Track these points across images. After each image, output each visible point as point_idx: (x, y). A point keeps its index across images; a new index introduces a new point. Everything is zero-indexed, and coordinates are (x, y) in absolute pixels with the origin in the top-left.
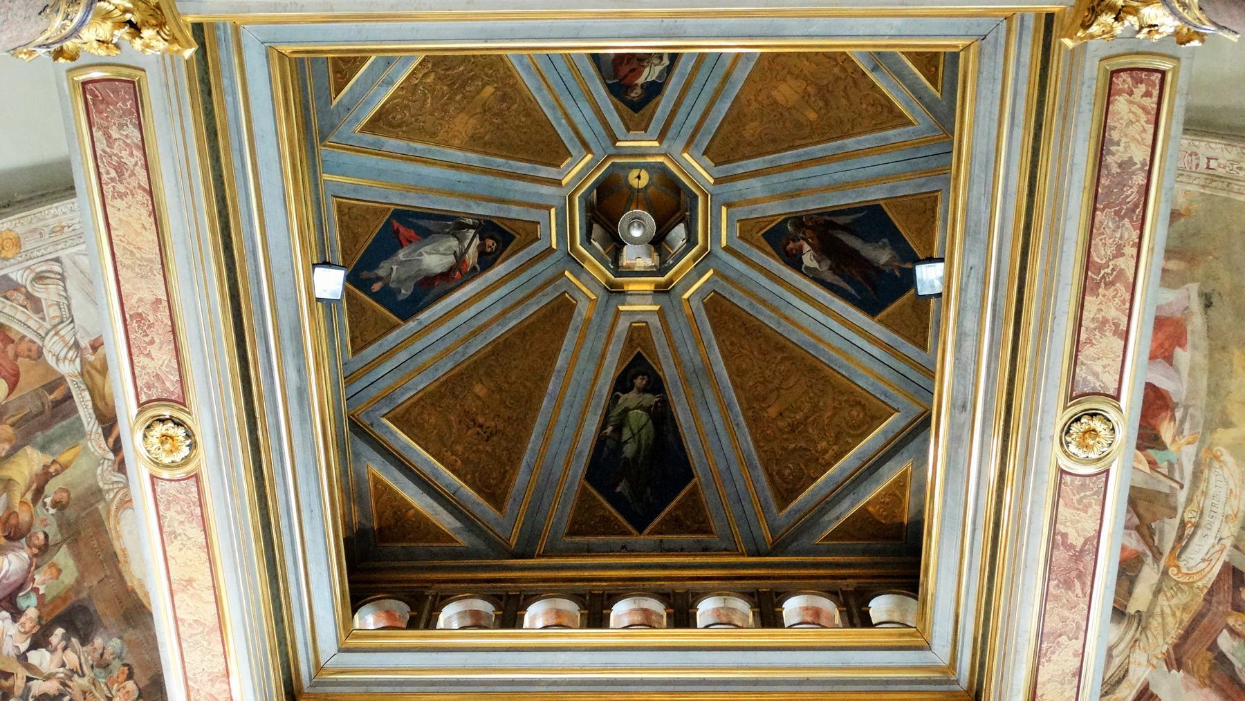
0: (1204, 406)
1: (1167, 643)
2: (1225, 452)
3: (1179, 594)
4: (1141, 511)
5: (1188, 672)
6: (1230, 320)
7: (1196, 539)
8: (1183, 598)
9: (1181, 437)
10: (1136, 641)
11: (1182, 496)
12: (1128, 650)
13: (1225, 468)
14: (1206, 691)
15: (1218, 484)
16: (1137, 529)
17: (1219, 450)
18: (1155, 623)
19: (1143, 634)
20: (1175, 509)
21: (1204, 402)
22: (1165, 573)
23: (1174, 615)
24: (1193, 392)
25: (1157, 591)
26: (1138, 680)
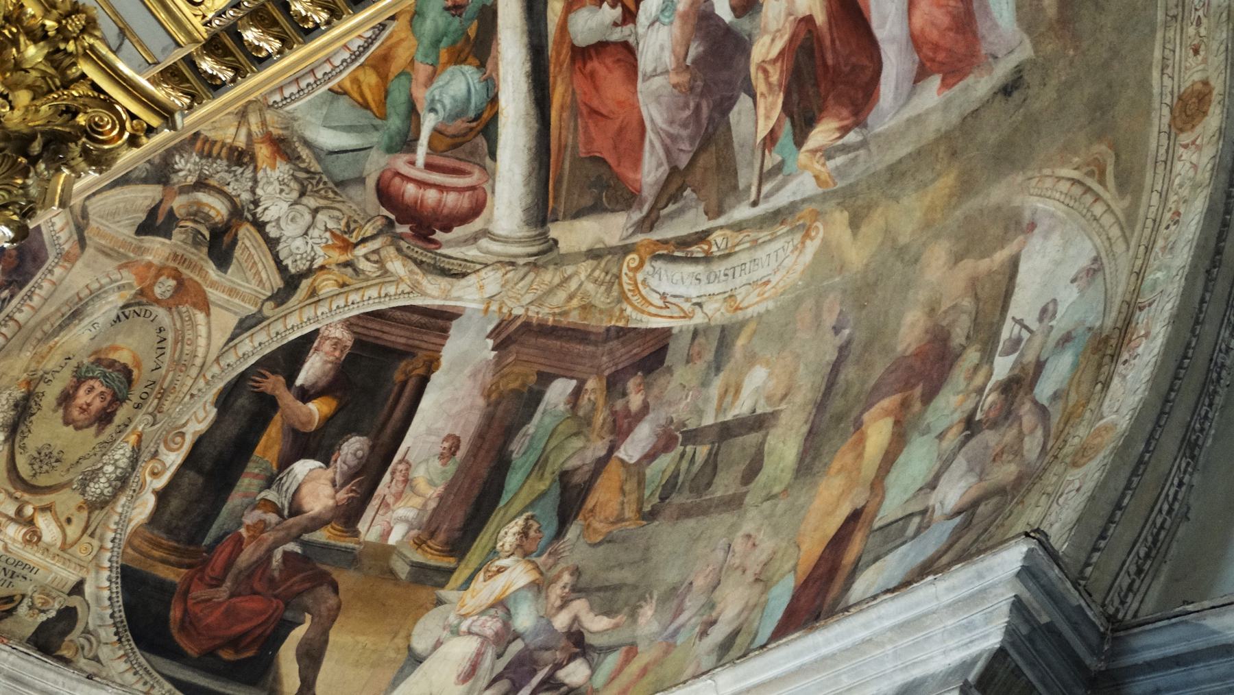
0: (872, 170)
1: (527, 310)
2: (817, 242)
3: (603, 288)
4: (701, 162)
5: (498, 362)
6: (993, 138)
7: (689, 269)
8: (600, 298)
9: (822, 160)
10: (513, 264)
11: (742, 212)
12: (495, 259)
13: (796, 253)
14: (481, 402)
15: (773, 257)
16: (674, 170)
18: (549, 277)
19: (526, 269)
20: (720, 212)
21: (879, 167)
22: (626, 250)
24: (888, 139)
25: (594, 254)
26: (459, 299)
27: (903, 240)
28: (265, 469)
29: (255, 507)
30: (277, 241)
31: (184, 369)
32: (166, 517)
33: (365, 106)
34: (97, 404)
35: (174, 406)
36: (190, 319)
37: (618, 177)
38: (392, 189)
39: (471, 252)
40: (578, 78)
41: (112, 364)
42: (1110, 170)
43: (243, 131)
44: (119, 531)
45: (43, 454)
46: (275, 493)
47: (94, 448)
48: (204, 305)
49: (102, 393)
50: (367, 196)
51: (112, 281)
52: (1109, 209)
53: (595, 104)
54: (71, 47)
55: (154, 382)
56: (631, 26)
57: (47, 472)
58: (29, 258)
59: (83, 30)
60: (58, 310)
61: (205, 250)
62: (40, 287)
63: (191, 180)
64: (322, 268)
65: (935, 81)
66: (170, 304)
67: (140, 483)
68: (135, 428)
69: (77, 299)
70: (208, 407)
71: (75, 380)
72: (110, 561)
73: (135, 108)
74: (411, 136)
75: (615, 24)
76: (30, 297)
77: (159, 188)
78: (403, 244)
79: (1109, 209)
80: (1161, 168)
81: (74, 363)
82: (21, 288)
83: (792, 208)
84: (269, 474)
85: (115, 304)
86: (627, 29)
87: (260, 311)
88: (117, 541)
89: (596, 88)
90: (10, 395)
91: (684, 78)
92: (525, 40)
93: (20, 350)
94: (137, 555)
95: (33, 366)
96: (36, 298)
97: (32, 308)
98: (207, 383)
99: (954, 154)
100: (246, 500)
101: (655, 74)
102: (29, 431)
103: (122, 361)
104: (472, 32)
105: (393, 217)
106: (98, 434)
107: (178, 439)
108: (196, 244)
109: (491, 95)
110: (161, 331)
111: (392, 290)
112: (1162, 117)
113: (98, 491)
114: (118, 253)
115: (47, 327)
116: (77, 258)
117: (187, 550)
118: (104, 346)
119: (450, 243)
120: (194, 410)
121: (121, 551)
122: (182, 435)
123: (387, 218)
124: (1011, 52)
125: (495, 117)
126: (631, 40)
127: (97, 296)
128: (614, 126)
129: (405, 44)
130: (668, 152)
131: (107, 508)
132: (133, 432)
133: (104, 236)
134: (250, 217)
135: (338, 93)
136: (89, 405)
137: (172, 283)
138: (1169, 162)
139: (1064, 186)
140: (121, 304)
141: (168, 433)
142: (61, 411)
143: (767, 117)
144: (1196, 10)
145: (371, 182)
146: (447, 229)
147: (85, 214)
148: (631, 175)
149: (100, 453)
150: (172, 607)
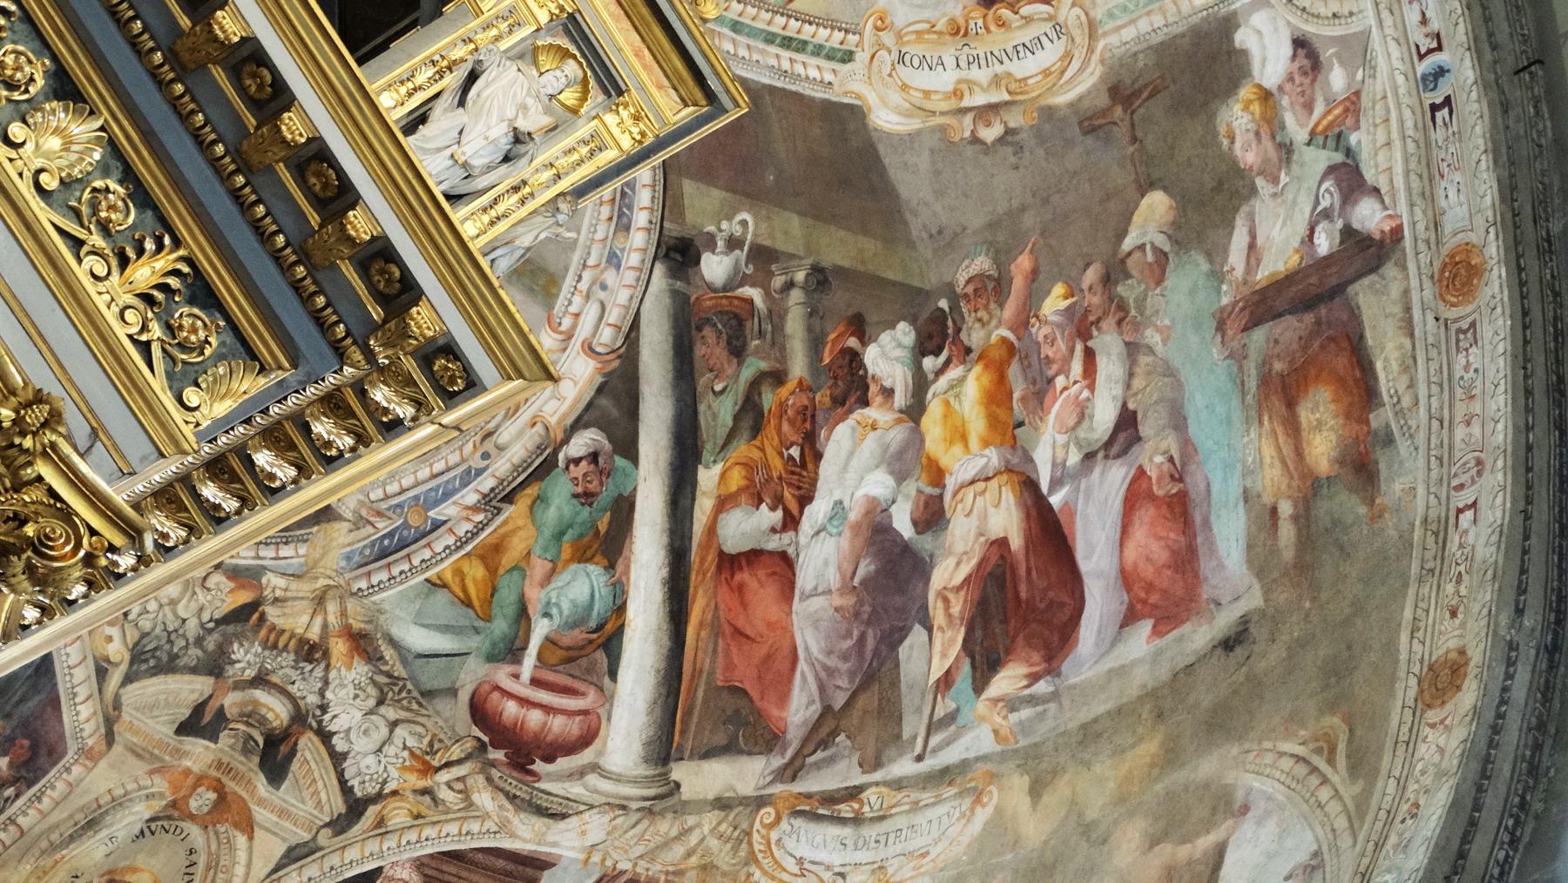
0: (1062, 729)
1: (635, 865)
2: (989, 810)
3: (729, 846)
4: (861, 702)
9: (1004, 712)
10: (624, 807)
11: (904, 767)
12: (604, 800)
13: (963, 821)
15: (935, 825)
16: (827, 710)
17: (993, 797)
18: (666, 826)
19: (639, 815)
20: (877, 765)
21: (1070, 725)
22: (760, 802)
23: (689, 854)
24: (1085, 692)
25: (722, 804)
26: (555, 844)
27: (1091, 814)
30: (344, 756)
33: (467, 603)
36: (229, 841)
37: (759, 714)
38: (488, 705)
39: (575, 790)
40: (724, 591)
42: (1342, 747)
43: (318, 621)
48: (247, 826)
50: (459, 711)
51: (140, 788)
52: (1337, 794)
53: (740, 622)
54: (28, 442)
56: (791, 534)
58: (43, 751)
59: (45, 425)
60: (71, 816)
61: (256, 759)
62: (53, 787)
63: (250, 674)
64: (395, 793)
65: (1146, 626)
66: (206, 822)
73: (96, 522)
74: (518, 644)
75: (773, 530)
76: (39, 799)
77: (210, 680)
78: (495, 773)
79: (1337, 794)
80: (1401, 749)
82: (29, 787)
83: (964, 766)
86: (788, 537)
87: (314, 839)
89: (744, 605)
91: (849, 601)
92: (665, 540)
93: (19, 861)
96: (46, 800)
97: (40, 811)
99: (1160, 715)
101: (815, 593)
104: (603, 526)
105: (486, 739)
108: (246, 751)
109: (619, 602)
111: (475, 827)
112: (1407, 689)
114: (152, 754)
115: (55, 837)
116: (101, 756)
118: (122, 865)
119: (552, 777)
123: (479, 739)
124: (1237, 599)
125: (620, 630)
126: (791, 551)
127: (120, 804)
128: (761, 651)
129: (522, 534)
130: (822, 688)
133: (137, 733)
134: (314, 724)
135: (437, 585)
137: (212, 796)
138: (1411, 743)
139: (1287, 764)
140: (147, 816)
143: (944, 655)
144: (1457, 564)
145: (464, 696)
146: (549, 759)
147: (117, 705)
148: (775, 712)
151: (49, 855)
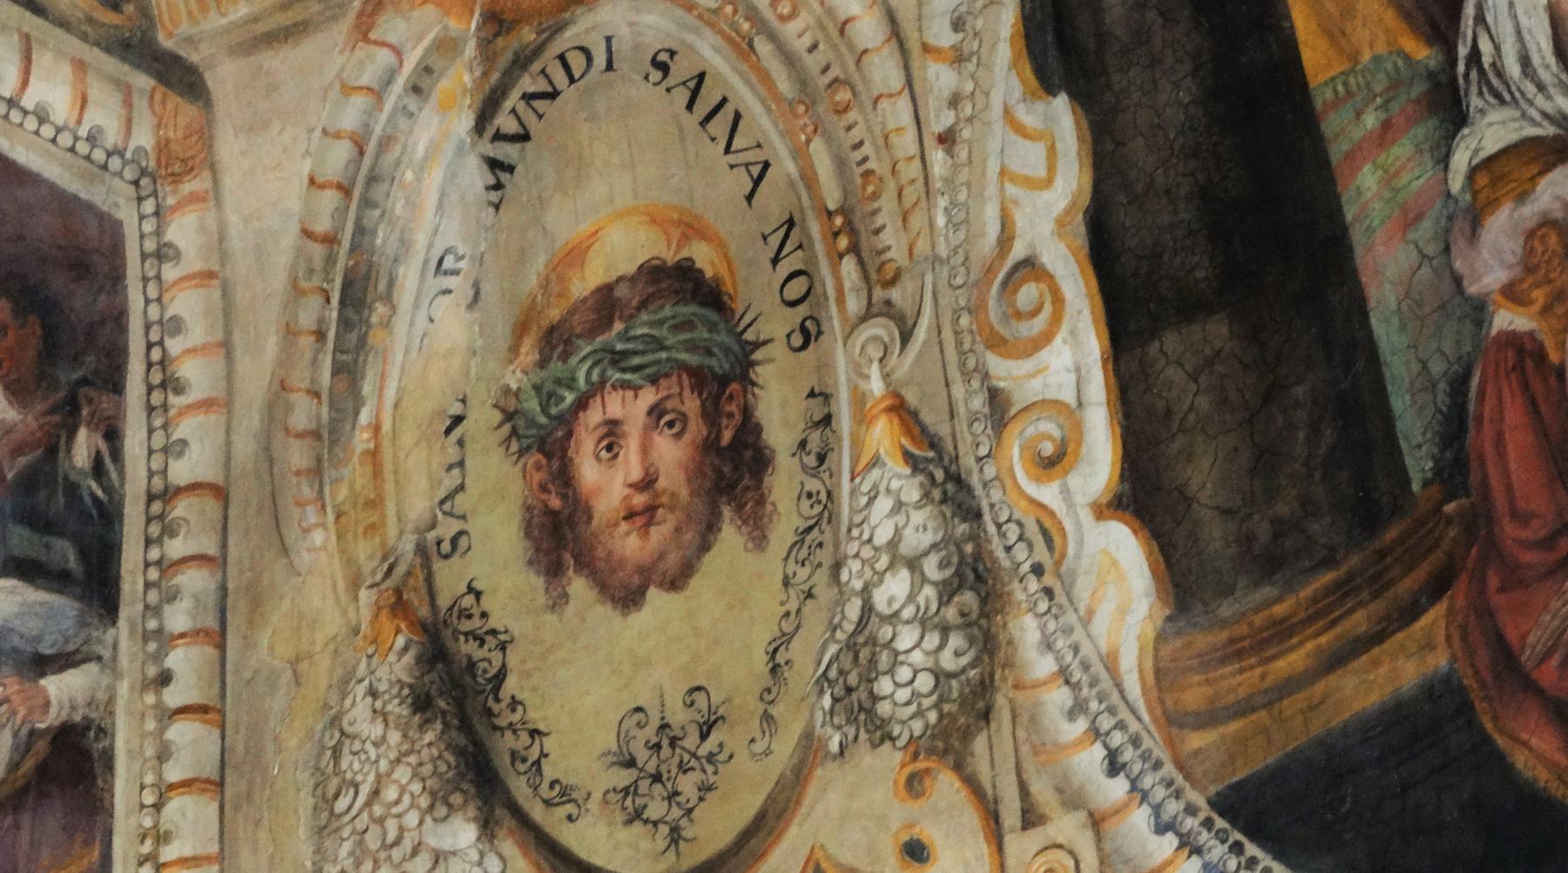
28: (1395, 84)
29: (1476, 218)
31: (843, 95)
32: (1215, 535)
34: (671, 454)
35: (917, 220)
41: (606, 303)
44: (1106, 723)
45: (642, 755)
46: (1495, 115)
47: (786, 583)
49: (656, 412)
51: (377, 94)
55: (791, 223)
57: (705, 788)
58: (58, 282)
60: (290, 332)
62: (175, 326)
67: (1032, 530)
68: (859, 398)
69: (318, 251)
70: (1029, 116)
71: (535, 457)
72: (1161, 828)
76: (172, 384)
81: (483, 419)
82: (116, 386)
84: (1419, 88)
85: (449, 149)
88: (1128, 755)
90: (373, 693)
93: (285, 550)
94: (1235, 726)
95: (365, 552)
96: (188, 370)
97: (207, 405)
98: (958, 57)
100: (1426, 230)
102: (534, 733)
103: (630, 268)
106: (759, 539)
107: (1028, 294)
110: (664, 68)
113: (925, 682)
115: (303, 413)
116: (205, 136)
117: (1382, 554)
118: (531, 281)
120: (993, 168)
121: (1169, 769)
122: (1030, 267)
127: (372, 179)
131: (1001, 701)
132: (862, 417)
136: (647, 483)
140: (464, 122)
141: (977, 309)
142: (579, 586)
149: (822, 577)
150: (1501, 741)
151: (336, 464)
